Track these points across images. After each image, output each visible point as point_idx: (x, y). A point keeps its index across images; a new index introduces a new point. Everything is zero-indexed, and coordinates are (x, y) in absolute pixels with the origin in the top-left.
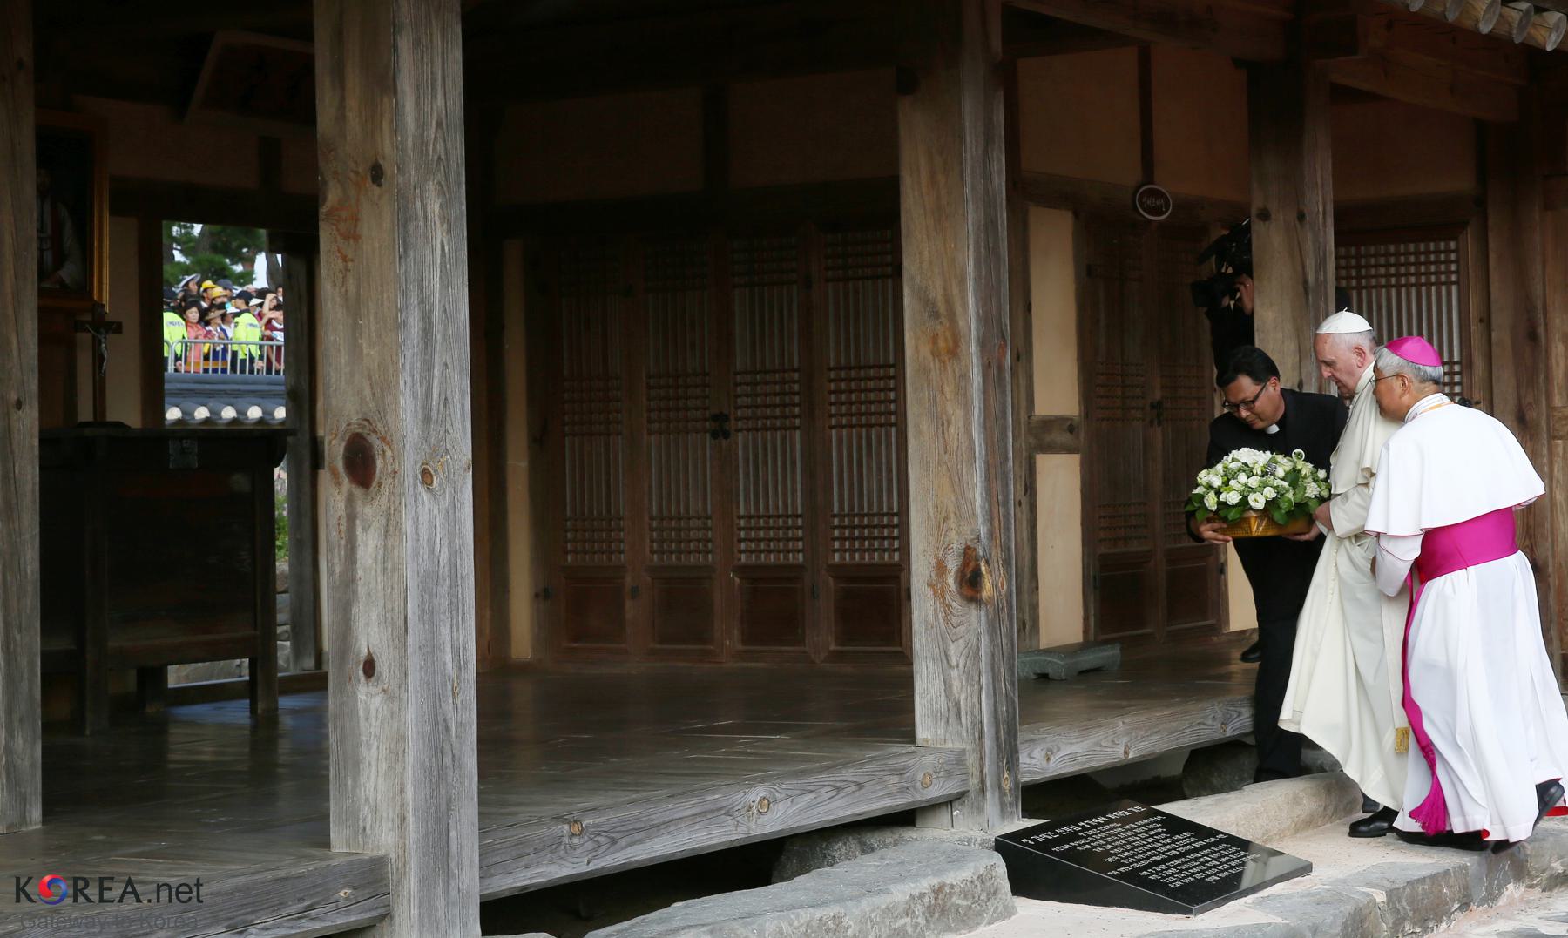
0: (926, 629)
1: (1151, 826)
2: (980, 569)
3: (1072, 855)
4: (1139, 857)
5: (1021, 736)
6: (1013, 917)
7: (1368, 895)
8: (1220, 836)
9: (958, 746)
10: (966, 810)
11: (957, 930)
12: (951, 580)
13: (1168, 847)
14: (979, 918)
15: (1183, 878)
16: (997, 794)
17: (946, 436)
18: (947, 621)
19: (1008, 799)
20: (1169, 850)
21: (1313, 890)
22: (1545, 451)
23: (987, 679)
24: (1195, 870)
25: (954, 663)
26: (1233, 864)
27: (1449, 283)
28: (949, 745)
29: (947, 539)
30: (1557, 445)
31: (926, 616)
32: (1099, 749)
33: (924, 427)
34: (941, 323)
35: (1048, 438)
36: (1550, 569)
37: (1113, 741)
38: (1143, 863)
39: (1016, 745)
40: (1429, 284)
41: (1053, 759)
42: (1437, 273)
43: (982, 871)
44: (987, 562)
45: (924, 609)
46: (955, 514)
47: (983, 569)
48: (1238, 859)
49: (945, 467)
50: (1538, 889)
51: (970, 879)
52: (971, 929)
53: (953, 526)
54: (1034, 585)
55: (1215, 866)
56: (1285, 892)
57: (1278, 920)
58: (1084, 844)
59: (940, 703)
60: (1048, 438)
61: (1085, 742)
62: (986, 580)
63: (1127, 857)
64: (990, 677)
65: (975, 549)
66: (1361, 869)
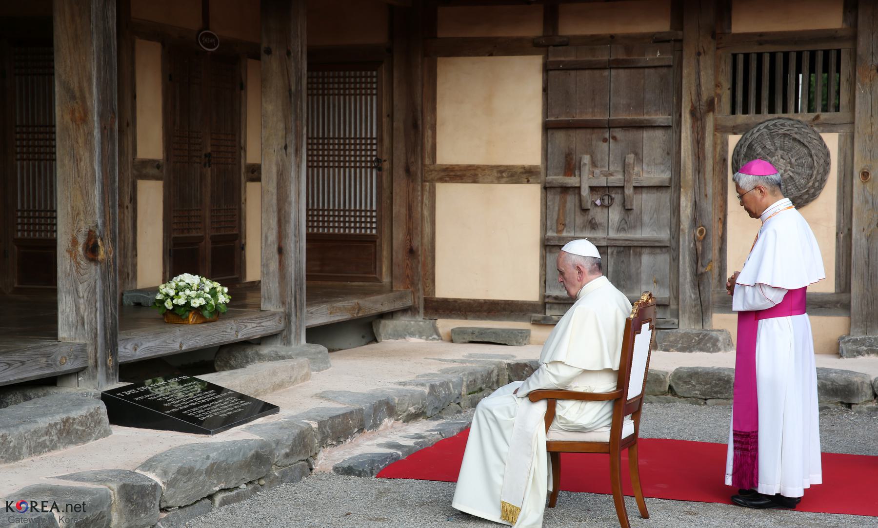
0: (65, 276)
1: (191, 387)
2: (97, 243)
3: (146, 402)
4: (183, 403)
5: (119, 337)
6: (110, 436)
7: (308, 424)
8: (230, 392)
9: (83, 341)
10: (86, 377)
11: (76, 443)
12: (80, 249)
13: (200, 398)
14: (90, 436)
15: (207, 415)
16: (104, 368)
17: (79, 168)
18: (78, 272)
19: (111, 371)
20: (201, 400)
21: (278, 422)
22: (419, 188)
23: (100, 304)
24: (214, 411)
25: (81, 295)
26: (236, 407)
27: (372, 95)
28: (78, 341)
29: (79, 226)
30: (425, 185)
31: (66, 269)
32: (165, 344)
33: (66, 162)
34: (77, 103)
35: (144, 171)
36: (420, 252)
37: (173, 341)
38: (185, 407)
39: (116, 342)
40: (361, 94)
41: (138, 350)
42: (366, 89)
43: (92, 410)
44: (102, 239)
45: (64, 264)
46: (84, 211)
47: (99, 243)
48: (239, 405)
49: (78, 185)
50: (401, 421)
51: (85, 415)
52: (84, 442)
53: (82, 218)
54: (135, 253)
55: (225, 409)
56: (264, 422)
57: (258, 437)
58: (152, 396)
59: (72, 318)
60: (144, 171)
61: (157, 341)
62: (101, 250)
63: (176, 404)
64: (102, 303)
65: (95, 232)
66: (306, 411)
